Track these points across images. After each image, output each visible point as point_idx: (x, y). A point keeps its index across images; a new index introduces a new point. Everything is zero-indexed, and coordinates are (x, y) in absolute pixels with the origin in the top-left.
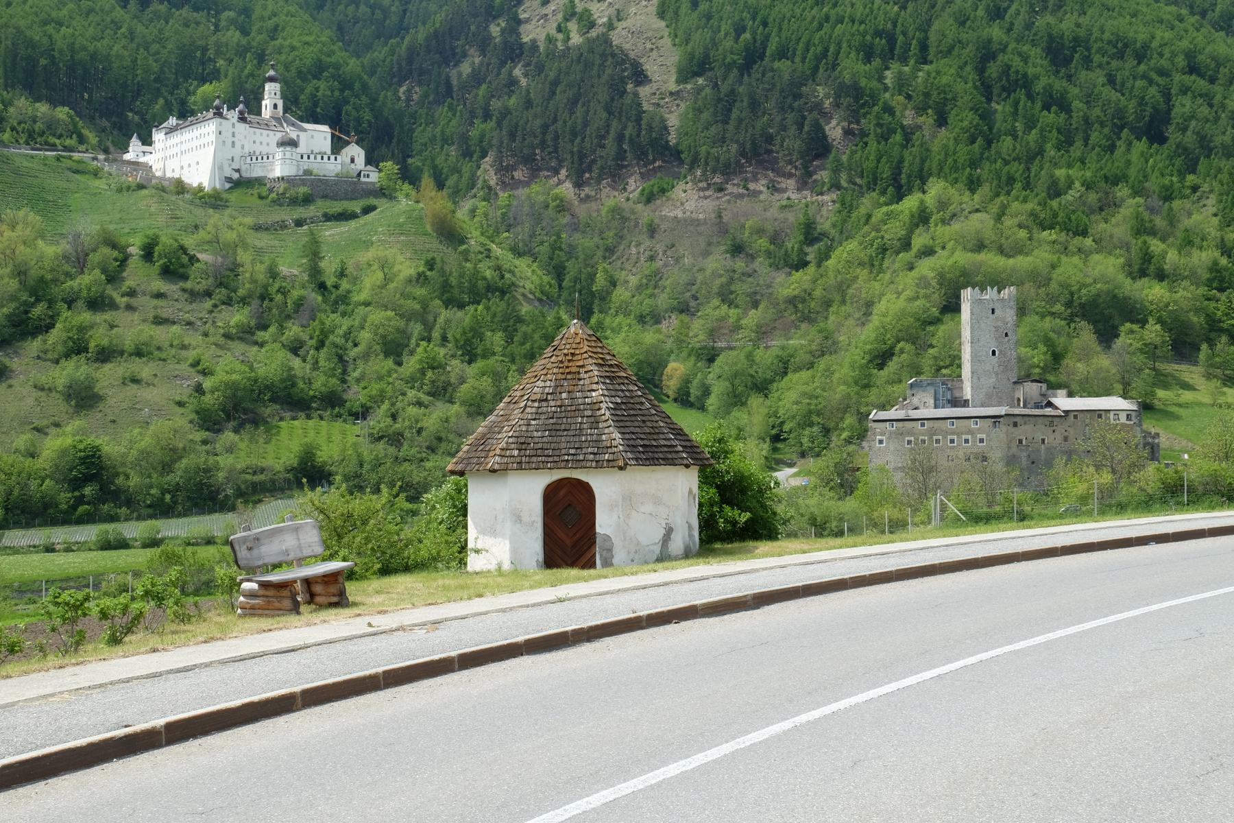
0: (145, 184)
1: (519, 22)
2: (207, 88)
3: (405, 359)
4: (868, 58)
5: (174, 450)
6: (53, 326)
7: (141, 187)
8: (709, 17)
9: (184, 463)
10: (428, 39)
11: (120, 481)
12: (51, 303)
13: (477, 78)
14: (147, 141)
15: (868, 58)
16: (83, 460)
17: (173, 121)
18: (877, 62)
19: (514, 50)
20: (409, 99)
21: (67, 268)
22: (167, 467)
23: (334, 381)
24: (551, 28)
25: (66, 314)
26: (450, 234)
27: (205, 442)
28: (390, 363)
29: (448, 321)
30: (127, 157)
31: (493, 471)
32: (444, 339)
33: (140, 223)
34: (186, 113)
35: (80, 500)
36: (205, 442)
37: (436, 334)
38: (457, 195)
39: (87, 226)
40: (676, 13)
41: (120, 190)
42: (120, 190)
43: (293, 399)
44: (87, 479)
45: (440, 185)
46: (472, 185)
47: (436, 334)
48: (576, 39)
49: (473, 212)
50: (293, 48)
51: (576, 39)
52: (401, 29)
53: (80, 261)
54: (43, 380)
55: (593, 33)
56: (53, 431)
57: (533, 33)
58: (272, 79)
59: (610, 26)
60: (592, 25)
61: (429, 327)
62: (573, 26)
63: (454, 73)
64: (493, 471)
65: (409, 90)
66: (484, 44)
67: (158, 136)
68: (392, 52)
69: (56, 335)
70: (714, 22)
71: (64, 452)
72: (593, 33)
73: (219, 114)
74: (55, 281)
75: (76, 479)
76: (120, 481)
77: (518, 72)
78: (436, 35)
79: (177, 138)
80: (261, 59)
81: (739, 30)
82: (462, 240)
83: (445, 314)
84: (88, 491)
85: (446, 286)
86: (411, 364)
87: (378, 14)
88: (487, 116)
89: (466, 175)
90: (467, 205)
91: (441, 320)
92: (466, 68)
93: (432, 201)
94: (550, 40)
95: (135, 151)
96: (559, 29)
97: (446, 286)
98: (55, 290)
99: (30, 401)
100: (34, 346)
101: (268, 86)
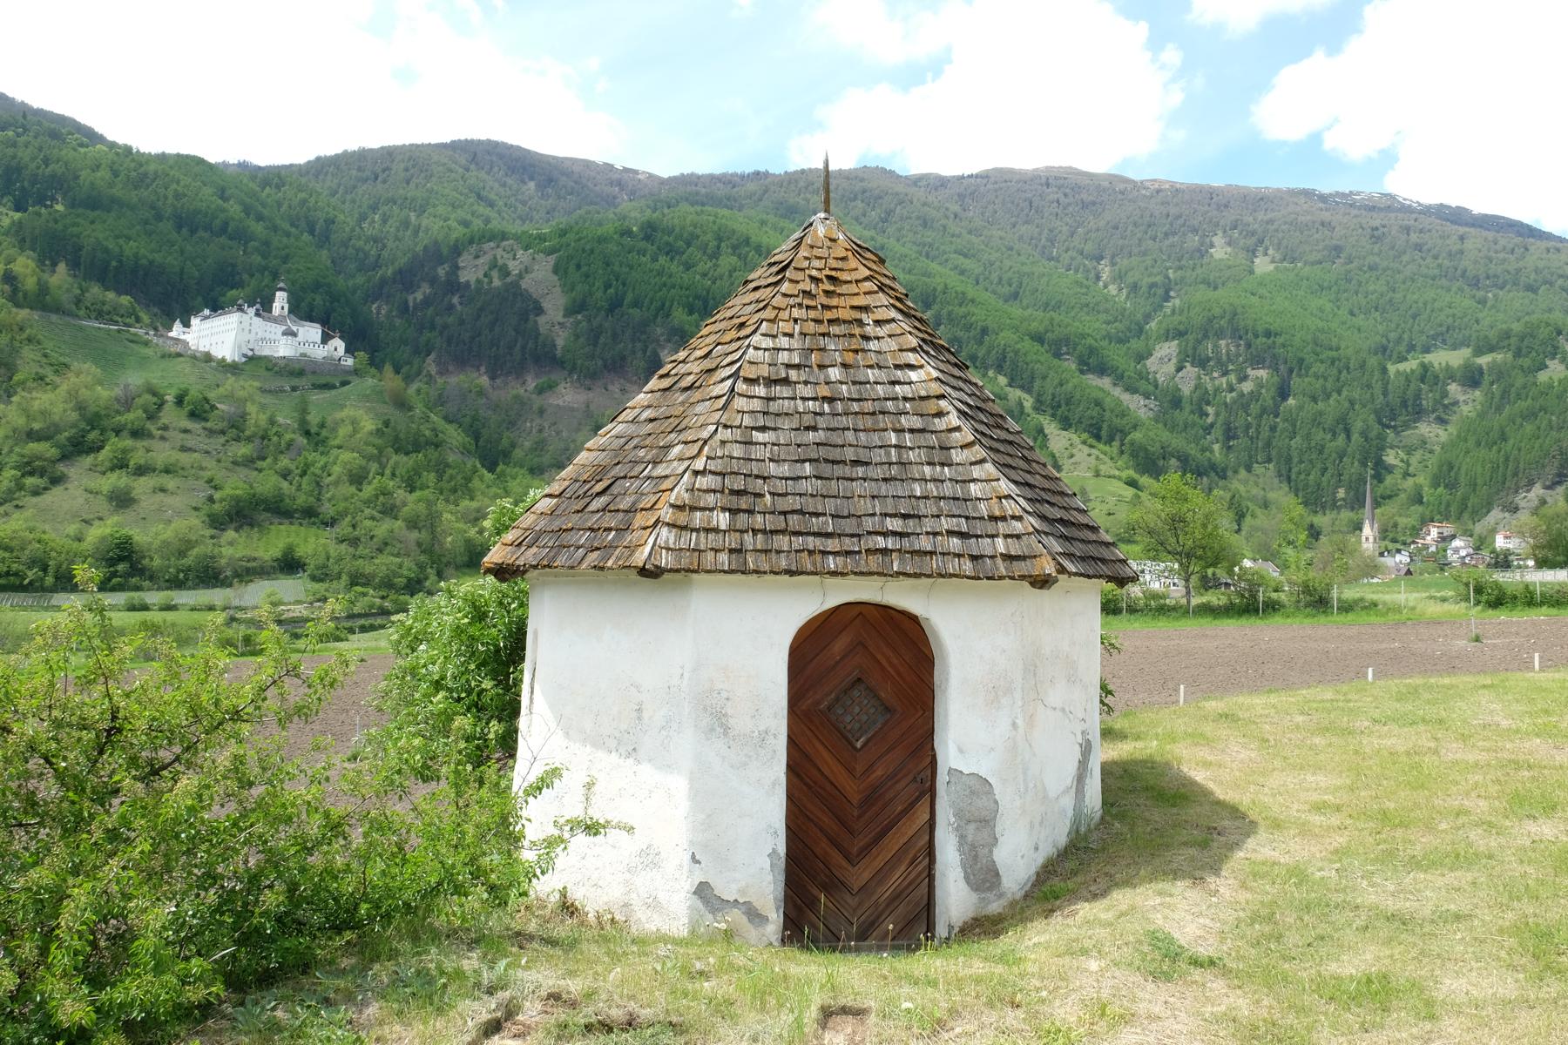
0: (181, 354)
1: (458, 268)
2: (234, 292)
3: (364, 487)
4: (691, 313)
5: (189, 541)
6: (102, 448)
7: (179, 355)
8: (587, 276)
9: (195, 551)
10: (394, 274)
11: (146, 562)
12: (103, 431)
13: (427, 302)
14: (187, 324)
15: (691, 313)
16: (118, 546)
17: (207, 312)
18: (696, 316)
19: (453, 286)
20: (378, 313)
21: (117, 406)
22: (182, 554)
23: (312, 499)
24: (480, 275)
25: (114, 440)
26: (402, 404)
27: (212, 537)
28: (353, 489)
29: (397, 463)
30: (171, 334)
31: (649, 573)
32: (393, 475)
33: (171, 379)
34: (217, 307)
35: (114, 574)
36: (212, 537)
37: (388, 472)
38: (408, 379)
39: (135, 379)
40: (566, 273)
41: (163, 356)
42: (163, 356)
43: (279, 509)
44: (121, 559)
45: (397, 372)
46: (419, 373)
47: (388, 472)
48: (497, 283)
49: (418, 391)
50: (299, 271)
51: (497, 283)
52: (376, 266)
53: (127, 403)
54: (92, 485)
55: (509, 280)
56: (97, 523)
57: (464, 276)
58: (281, 289)
59: (520, 276)
60: (508, 274)
61: (383, 467)
62: (495, 274)
63: (410, 299)
64: (649, 573)
65: (379, 308)
66: (433, 281)
67: (195, 321)
68: (368, 281)
69: (105, 453)
70: (591, 280)
71: (103, 539)
72: (509, 280)
73: (240, 309)
74: (108, 416)
75: (112, 559)
76: (146, 562)
77: (455, 300)
78: (400, 271)
79: (208, 323)
80: (275, 276)
81: (608, 286)
82: (410, 409)
83: (395, 458)
84: (121, 567)
85: (397, 439)
86: (368, 490)
87: (361, 255)
88: (433, 327)
89: (416, 366)
90: (414, 387)
91: (391, 462)
92: (419, 296)
93: (390, 380)
94: (478, 281)
95: (177, 331)
96: (485, 275)
97: (397, 439)
98: (105, 423)
99: (81, 501)
100: (88, 460)
101: (278, 294)
